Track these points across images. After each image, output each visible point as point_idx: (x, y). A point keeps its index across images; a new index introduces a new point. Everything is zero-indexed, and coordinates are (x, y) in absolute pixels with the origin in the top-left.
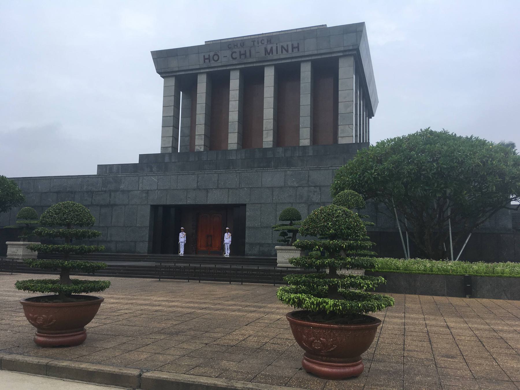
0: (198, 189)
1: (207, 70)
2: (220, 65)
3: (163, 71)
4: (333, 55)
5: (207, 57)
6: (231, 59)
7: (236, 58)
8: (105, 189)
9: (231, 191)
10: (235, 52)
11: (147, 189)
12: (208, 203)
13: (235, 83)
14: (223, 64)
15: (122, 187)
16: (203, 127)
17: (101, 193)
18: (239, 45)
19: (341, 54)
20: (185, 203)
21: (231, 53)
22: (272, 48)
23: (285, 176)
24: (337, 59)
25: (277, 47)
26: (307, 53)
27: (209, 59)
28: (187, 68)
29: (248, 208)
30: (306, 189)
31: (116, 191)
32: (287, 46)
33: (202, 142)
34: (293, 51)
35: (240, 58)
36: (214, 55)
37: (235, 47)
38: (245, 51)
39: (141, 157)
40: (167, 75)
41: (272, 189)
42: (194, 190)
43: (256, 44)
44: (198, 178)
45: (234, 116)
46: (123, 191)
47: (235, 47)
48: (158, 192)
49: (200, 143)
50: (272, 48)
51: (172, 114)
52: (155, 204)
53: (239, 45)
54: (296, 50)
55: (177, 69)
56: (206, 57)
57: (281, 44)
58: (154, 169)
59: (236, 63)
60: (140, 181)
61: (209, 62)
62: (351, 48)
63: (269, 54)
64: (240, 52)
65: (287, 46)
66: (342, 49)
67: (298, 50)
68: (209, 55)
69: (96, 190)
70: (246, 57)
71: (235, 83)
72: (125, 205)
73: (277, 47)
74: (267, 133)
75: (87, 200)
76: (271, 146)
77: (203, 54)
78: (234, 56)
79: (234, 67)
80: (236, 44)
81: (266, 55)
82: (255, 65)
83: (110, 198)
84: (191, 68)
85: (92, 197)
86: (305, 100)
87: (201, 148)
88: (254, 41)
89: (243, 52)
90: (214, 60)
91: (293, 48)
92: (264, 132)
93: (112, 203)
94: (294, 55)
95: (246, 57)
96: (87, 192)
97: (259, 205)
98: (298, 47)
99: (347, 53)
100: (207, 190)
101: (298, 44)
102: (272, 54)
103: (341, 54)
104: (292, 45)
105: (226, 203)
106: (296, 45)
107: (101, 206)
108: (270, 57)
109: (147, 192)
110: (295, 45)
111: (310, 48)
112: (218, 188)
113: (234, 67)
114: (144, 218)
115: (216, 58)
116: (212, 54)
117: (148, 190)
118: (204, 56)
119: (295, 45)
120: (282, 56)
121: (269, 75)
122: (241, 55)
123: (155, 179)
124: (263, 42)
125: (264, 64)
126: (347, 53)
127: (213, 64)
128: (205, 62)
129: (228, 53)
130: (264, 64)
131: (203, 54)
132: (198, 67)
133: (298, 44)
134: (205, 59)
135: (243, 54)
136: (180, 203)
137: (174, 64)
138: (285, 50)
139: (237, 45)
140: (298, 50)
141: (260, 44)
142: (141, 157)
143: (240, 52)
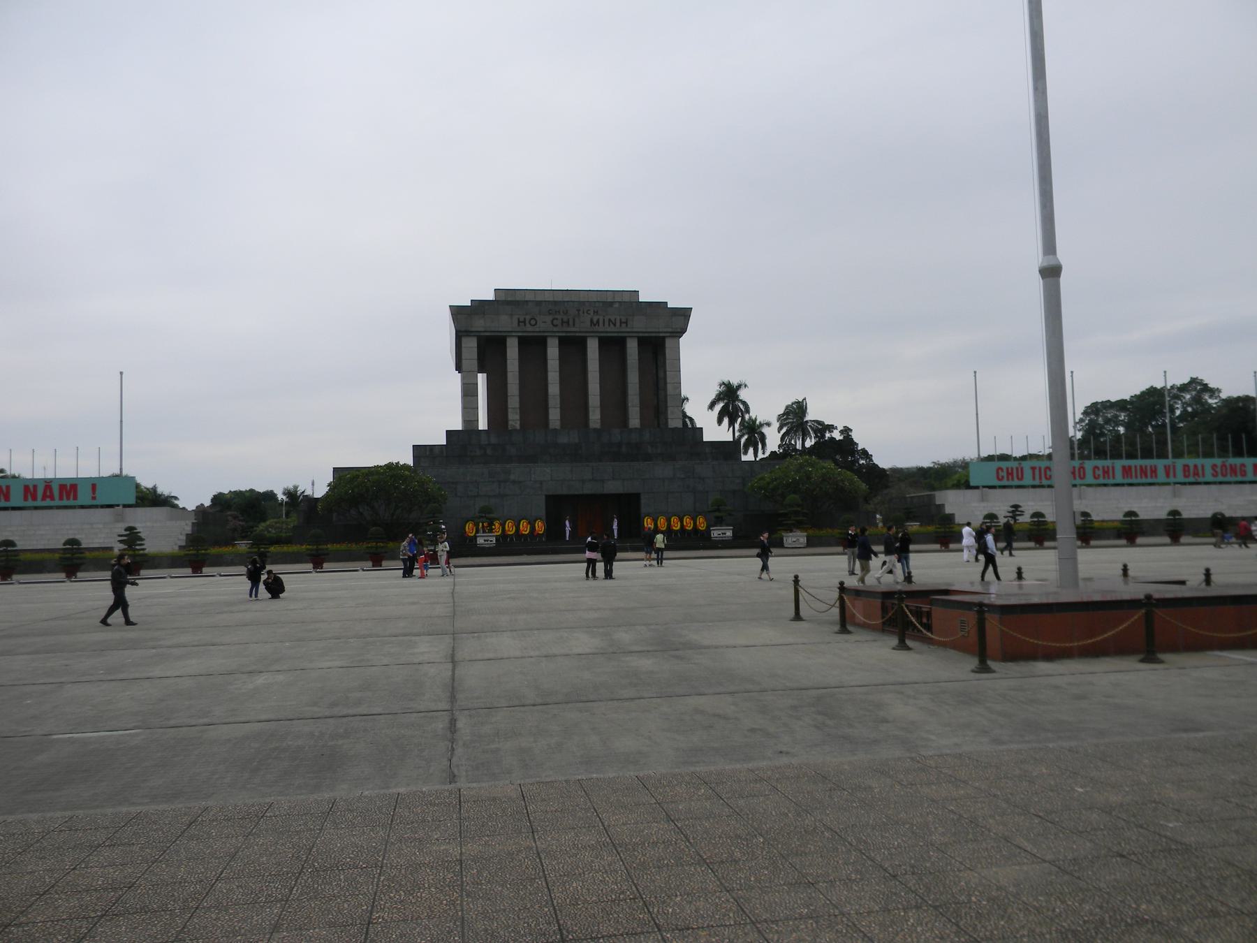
13: (553, 351)
15: (512, 477)
16: (517, 399)
24: (664, 338)
27: (524, 322)
33: (518, 417)
39: (450, 434)
45: (554, 389)
46: (514, 482)
49: (514, 419)
71: (553, 351)
76: (598, 426)
86: (633, 378)
98: (626, 323)
108: (596, 328)
109: (541, 483)
111: (640, 325)
114: (540, 507)
116: (528, 317)
121: (593, 347)
127: (529, 328)
137: (479, 324)
142: (450, 434)
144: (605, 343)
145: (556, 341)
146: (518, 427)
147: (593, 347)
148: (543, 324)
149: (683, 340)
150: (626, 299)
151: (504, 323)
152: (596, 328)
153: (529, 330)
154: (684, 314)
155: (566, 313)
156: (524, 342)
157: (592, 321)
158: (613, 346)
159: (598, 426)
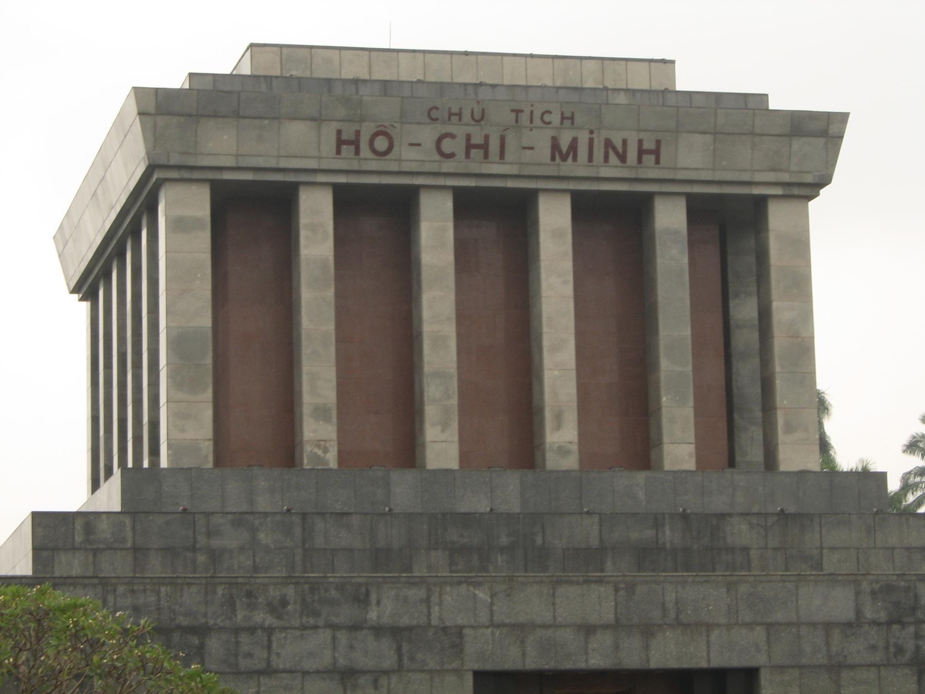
0: (617, 626)
1: (342, 179)
2: (396, 169)
3: (175, 160)
4: (757, 191)
5: (347, 135)
6: (437, 157)
7: (451, 156)
8: (312, 621)
9: (715, 633)
10: (453, 136)
11: (460, 621)
12: (653, 665)
14: (406, 167)
15: (373, 615)
17: (298, 633)
18: (467, 117)
19: (778, 191)
20: (582, 665)
21: (438, 135)
22: (574, 142)
23: (857, 594)
24: (760, 203)
25: (591, 141)
26: (681, 175)
27: (355, 142)
28: (272, 163)
29: (765, 678)
30: (911, 629)
31: (355, 628)
32: (625, 142)
34: (640, 160)
35: (468, 156)
36: (377, 134)
37: (454, 119)
38: (487, 137)
40: (186, 175)
41: (828, 626)
42: (606, 627)
43: (524, 118)
44: (617, 590)
46: (378, 631)
47: (454, 119)
48: (493, 634)
50: (574, 142)
51: (206, 321)
52: (489, 667)
53: (467, 117)
54: (649, 159)
55: (230, 162)
56: (345, 137)
57: (605, 134)
58: (261, 536)
59: (451, 170)
60: (435, 599)
61: (357, 152)
62: (809, 179)
63: (564, 158)
64: (468, 137)
65: (625, 142)
66: (785, 177)
67: (657, 161)
68: (358, 133)
69: (282, 623)
70: (486, 156)
72: (386, 673)
73: (591, 141)
74: (559, 418)
75: (250, 655)
76: (571, 462)
77: (335, 126)
78: (447, 145)
79: (441, 181)
80: (455, 110)
81: (553, 158)
82: (510, 184)
83: (334, 648)
84: (283, 164)
85: (269, 647)
87: (326, 451)
88: (518, 112)
89: (477, 140)
90: (374, 151)
91: (641, 152)
92: (548, 415)
93: (342, 662)
94: (643, 174)
95: (486, 156)
96: (252, 630)
97: (796, 672)
98: (657, 152)
99: (796, 191)
100: (648, 631)
101: (658, 142)
102: (575, 159)
103: (778, 191)
104: (640, 142)
105: (704, 664)
106: (652, 146)
107: (305, 673)
110: (649, 145)
111: (692, 158)
112: (678, 623)
113: (441, 181)
115: (381, 144)
117: (462, 627)
118: (339, 132)
119: (649, 145)
120: (605, 172)
121: (554, 219)
122: (469, 147)
123: (482, 595)
124: (547, 118)
125: (541, 185)
126: (796, 191)
128: (338, 152)
129: (427, 135)
130: (541, 185)
131: (335, 126)
132: (312, 164)
133: (658, 142)
134: (340, 142)
135: (477, 146)
136: (568, 666)
138: (617, 153)
139: (460, 115)
140: (657, 161)
141: (537, 121)
143: (468, 137)
144: (588, 209)
145: (446, 204)
146: (332, 459)
147: (554, 219)
148: (413, 155)
149: (819, 209)
150: (640, 82)
151: (292, 144)
152: (568, 168)
153: (372, 171)
154: (820, 133)
155: (479, 119)
156: (350, 202)
157: (555, 146)
158: (614, 222)
159: (571, 462)
